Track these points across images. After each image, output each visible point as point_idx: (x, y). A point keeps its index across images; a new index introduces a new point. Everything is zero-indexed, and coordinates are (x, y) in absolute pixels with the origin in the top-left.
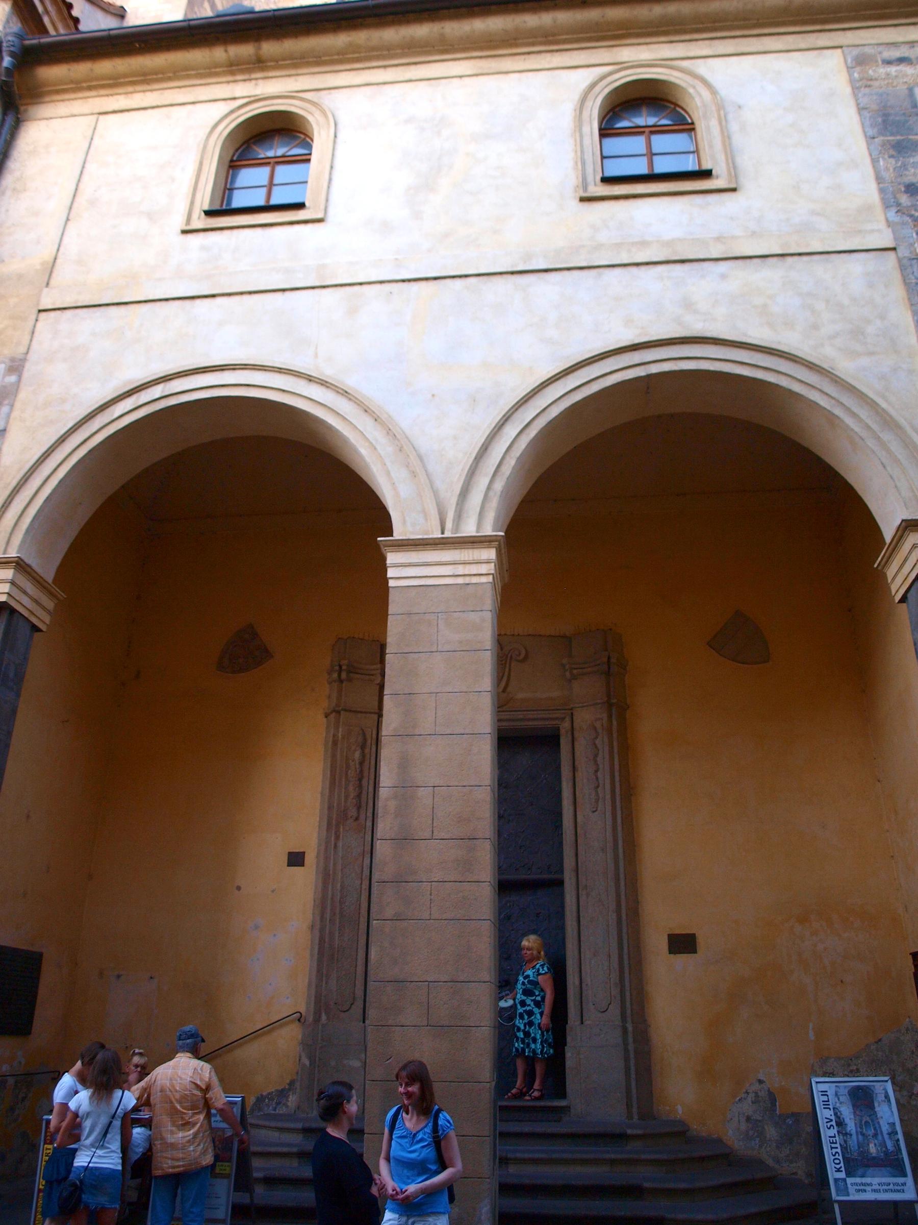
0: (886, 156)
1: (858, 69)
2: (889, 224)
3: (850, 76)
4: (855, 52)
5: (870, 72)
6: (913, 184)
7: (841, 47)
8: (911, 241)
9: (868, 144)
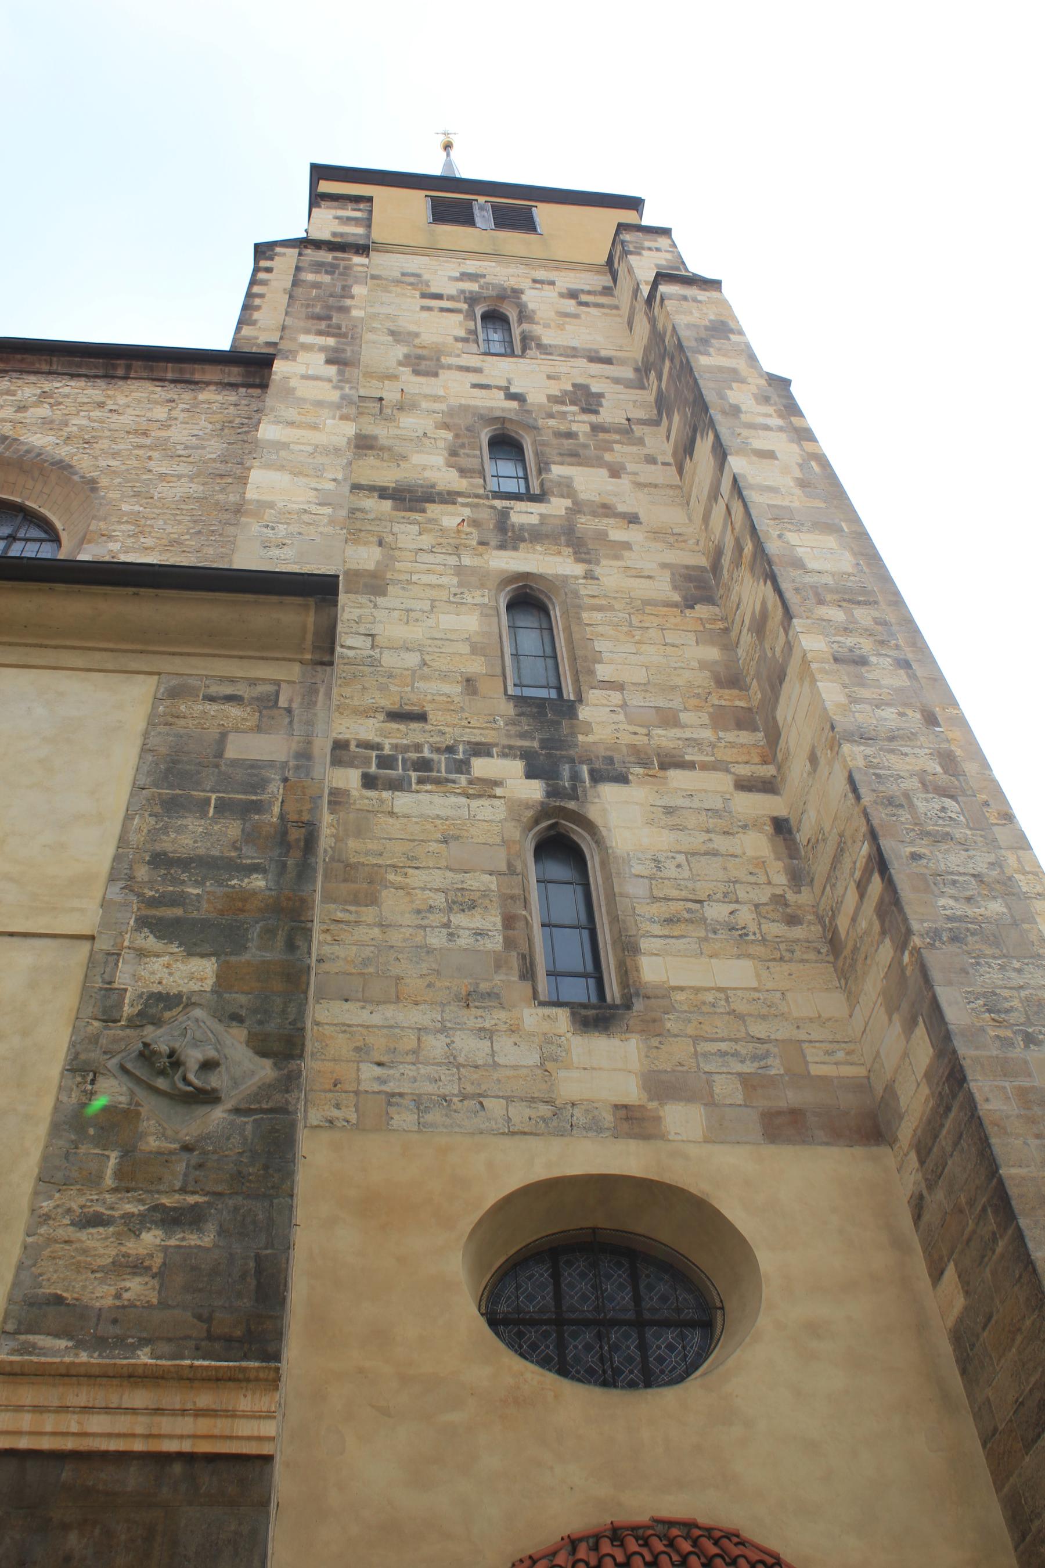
0: (146, 814)
1: (168, 702)
2: (104, 904)
3: (154, 707)
4: (174, 682)
5: (183, 708)
6: (165, 854)
7: (159, 674)
8: (124, 928)
9: (132, 795)
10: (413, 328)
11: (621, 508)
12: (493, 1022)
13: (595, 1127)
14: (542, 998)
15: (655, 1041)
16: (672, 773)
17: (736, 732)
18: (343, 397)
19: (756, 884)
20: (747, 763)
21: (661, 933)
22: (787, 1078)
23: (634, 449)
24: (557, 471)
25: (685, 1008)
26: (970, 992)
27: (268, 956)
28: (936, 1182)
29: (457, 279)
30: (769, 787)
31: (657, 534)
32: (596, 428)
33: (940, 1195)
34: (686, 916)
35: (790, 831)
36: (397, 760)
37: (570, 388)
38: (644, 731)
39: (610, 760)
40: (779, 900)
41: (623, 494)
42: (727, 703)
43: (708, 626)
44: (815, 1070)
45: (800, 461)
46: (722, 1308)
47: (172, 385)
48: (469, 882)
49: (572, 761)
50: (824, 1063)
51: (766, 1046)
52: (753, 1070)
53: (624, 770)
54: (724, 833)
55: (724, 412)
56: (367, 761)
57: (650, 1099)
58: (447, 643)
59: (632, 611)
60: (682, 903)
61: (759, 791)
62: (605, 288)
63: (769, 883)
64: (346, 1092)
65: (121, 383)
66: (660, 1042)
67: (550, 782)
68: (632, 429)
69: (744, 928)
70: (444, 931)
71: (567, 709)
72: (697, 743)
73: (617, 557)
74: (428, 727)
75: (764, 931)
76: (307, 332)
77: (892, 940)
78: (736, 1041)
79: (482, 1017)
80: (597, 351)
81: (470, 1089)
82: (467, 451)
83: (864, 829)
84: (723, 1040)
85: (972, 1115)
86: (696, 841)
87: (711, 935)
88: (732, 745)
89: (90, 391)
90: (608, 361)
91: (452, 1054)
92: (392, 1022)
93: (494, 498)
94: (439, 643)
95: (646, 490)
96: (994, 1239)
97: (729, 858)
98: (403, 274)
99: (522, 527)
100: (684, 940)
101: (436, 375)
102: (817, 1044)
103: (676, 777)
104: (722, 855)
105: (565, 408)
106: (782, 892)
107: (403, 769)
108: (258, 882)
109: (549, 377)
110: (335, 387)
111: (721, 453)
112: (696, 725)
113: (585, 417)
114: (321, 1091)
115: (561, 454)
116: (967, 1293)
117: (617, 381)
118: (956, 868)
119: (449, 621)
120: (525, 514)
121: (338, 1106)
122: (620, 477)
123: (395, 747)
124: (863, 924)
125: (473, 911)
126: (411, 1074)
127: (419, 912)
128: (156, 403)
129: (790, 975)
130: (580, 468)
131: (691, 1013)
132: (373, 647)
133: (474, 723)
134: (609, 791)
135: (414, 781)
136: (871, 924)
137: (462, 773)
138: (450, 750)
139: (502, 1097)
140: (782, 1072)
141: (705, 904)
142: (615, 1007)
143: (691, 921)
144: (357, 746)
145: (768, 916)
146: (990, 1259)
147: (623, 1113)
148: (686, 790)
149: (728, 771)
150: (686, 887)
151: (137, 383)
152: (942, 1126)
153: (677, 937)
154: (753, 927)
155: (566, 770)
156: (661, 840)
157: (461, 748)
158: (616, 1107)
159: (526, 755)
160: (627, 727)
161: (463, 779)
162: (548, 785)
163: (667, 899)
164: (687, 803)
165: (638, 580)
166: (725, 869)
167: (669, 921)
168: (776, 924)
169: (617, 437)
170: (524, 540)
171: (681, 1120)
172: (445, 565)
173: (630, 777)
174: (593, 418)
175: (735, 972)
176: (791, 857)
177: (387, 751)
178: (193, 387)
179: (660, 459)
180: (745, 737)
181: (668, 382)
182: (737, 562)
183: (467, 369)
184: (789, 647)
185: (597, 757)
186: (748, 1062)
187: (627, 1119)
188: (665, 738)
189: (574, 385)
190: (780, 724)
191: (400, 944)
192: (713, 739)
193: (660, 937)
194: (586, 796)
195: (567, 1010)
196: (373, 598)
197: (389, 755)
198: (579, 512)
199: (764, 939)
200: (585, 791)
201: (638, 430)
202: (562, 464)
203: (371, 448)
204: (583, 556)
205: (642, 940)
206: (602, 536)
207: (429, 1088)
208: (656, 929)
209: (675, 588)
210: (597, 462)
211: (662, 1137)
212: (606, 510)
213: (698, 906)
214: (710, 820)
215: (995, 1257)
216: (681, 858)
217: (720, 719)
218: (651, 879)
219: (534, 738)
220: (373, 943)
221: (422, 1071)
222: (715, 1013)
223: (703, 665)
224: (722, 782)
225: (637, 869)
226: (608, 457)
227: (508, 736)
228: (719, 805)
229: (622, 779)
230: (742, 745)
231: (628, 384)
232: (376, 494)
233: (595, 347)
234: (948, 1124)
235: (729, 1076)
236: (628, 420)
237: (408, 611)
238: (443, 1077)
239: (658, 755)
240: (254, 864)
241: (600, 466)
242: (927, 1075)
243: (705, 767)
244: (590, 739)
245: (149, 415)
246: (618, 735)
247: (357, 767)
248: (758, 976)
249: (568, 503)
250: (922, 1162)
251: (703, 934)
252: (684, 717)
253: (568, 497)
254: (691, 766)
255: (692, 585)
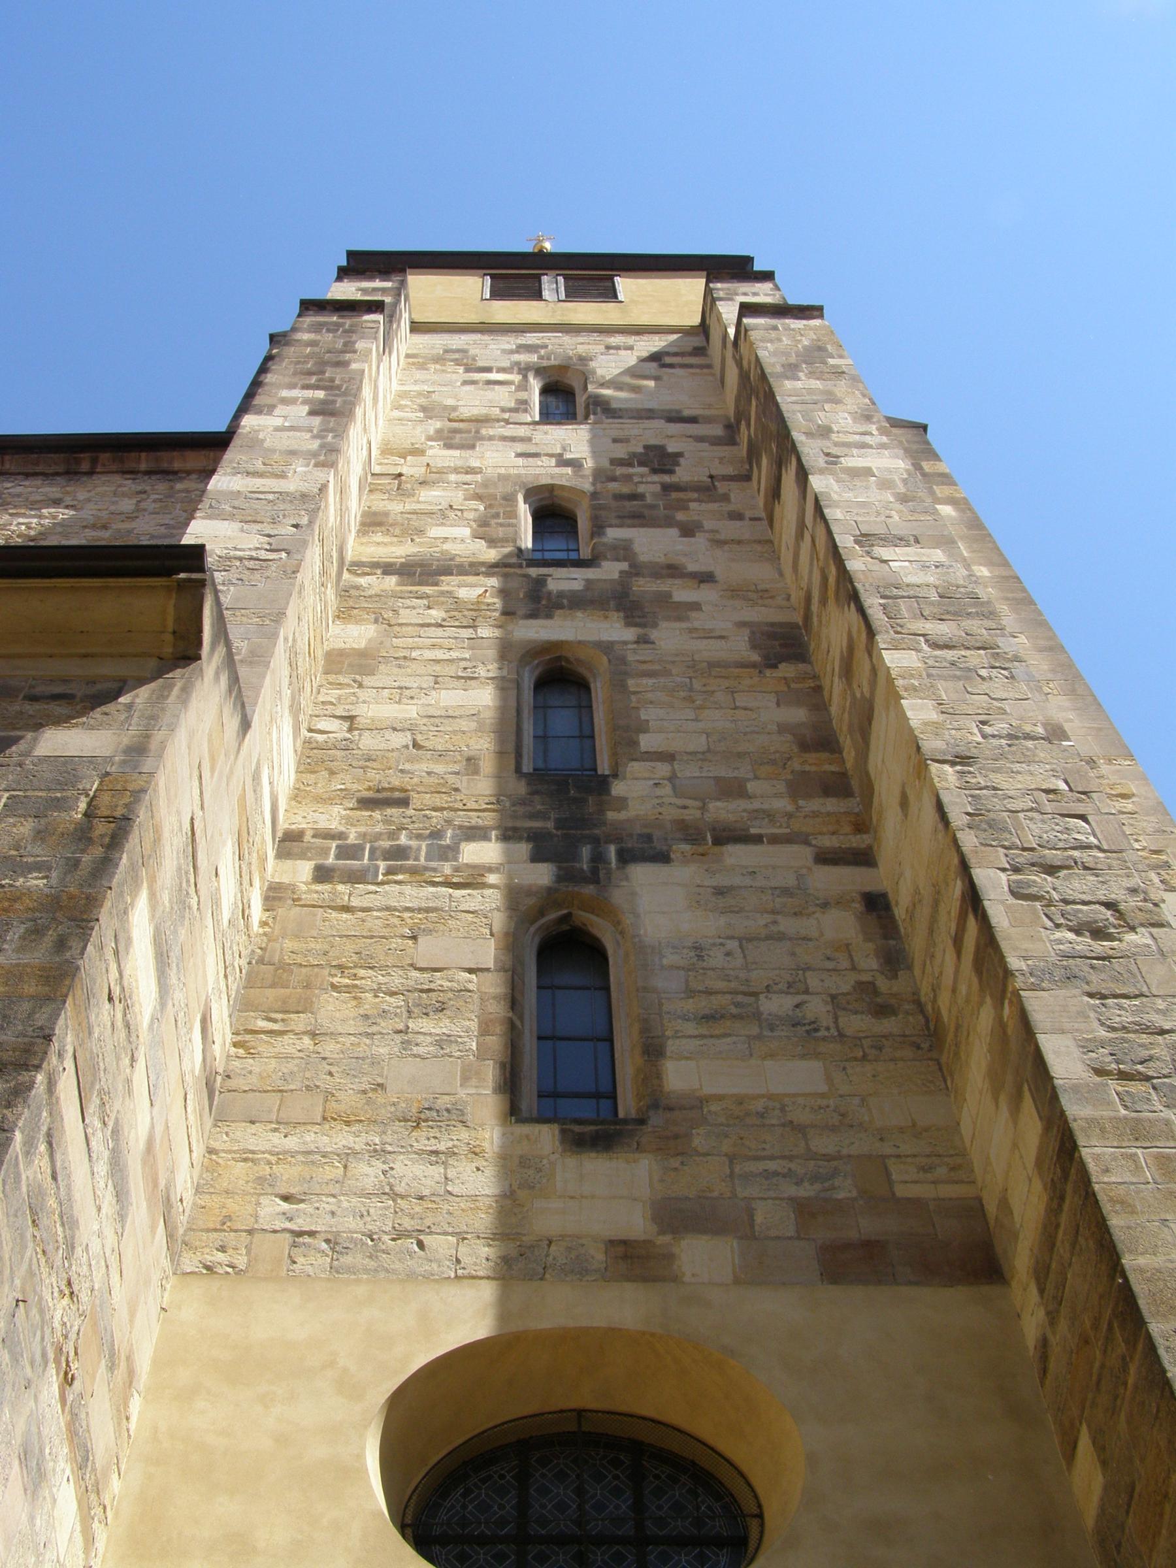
10: (450, 402)
11: (692, 567)
12: (450, 1144)
13: (578, 1269)
14: (525, 1114)
15: (675, 1162)
16: (730, 848)
17: (821, 800)
18: (322, 446)
19: (834, 970)
20: (833, 833)
21: (696, 1033)
22: (861, 1202)
23: (714, 506)
24: (613, 534)
25: (722, 1120)
26: (1090, 1040)
27: (26, 958)
28: (1058, 1311)
29: (512, 352)
30: (864, 858)
31: (736, 592)
32: (667, 488)
33: (1063, 1325)
34: (734, 1010)
35: (887, 907)
36: (363, 849)
37: (642, 450)
38: (698, 804)
39: (649, 838)
40: (866, 988)
41: (697, 554)
42: (813, 768)
43: (793, 686)
44: (901, 1191)
45: (905, 476)
46: (760, 1516)
47: (146, 478)
48: (439, 982)
49: (596, 841)
50: (916, 1182)
51: (835, 1163)
52: (812, 1194)
53: (665, 848)
54: (795, 914)
55: (809, 434)
56: (325, 852)
57: (662, 1232)
58: (446, 721)
59: (692, 674)
60: (728, 997)
61: (847, 863)
62: (696, 349)
63: (854, 968)
64: (236, 1231)
65: (85, 479)
66: (682, 1163)
67: (565, 865)
68: (714, 486)
69: (814, 1022)
70: (398, 1038)
71: (601, 785)
72: (770, 816)
73: (679, 619)
74: (410, 812)
75: (841, 1025)
76: (292, 386)
77: (991, 997)
78: (791, 1158)
79: (435, 1138)
80: (679, 411)
81: (408, 1224)
82: (501, 521)
83: (956, 861)
84: (772, 1158)
85: (1087, 1193)
86: (758, 923)
87: (766, 1033)
88: (815, 814)
89: (47, 489)
90: (693, 420)
91: (390, 1184)
92: (312, 1147)
93: (528, 566)
94: (437, 721)
95: (726, 547)
96: (1125, 1368)
97: (800, 942)
98: (446, 351)
99: (561, 594)
100: (729, 1040)
101: (473, 447)
102: (909, 1160)
103: (737, 855)
104: (790, 939)
105: (631, 470)
106: (870, 979)
107: (370, 859)
108: (36, 882)
109: (615, 441)
110: (314, 437)
111: (803, 475)
112: (769, 796)
113: (656, 478)
114: (202, 1230)
115: (619, 517)
116: (1104, 1463)
117: (700, 439)
118: (1081, 896)
119: (450, 698)
120: (564, 580)
121: (222, 1249)
122: (694, 536)
123: (363, 836)
124: (963, 989)
125: (440, 1015)
126: (328, 1208)
127: (366, 1017)
128: (124, 495)
129: (874, 1076)
130: (642, 530)
131: (728, 1126)
132: (350, 730)
133: (469, 806)
134: (641, 873)
135: (381, 871)
136: (970, 986)
137: (447, 860)
138: (436, 834)
139: (452, 1234)
140: (854, 1194)
141: (762, 997)
142: (625, 1121)
143: (739, 1017)
144: (313, 836)
145: (850, 1007)
146: (1123, 1399)
147: (621, 1250)
148: (746, 867)
149: (807, 843)
150: (737, 977)
151: (104, 478)
152: (1058, 1226)
153: (718, 1037)
154: (826, 1020)
155: (586, 851)
156: (707, 925)
157: (449, 833)
158: (612, 1243)
159: (535, 837)
160: (674, 800)
161: (447, 868)
162: (559, 868)
163: (709, 992)
164: (748, 881)
165: (705, 642)
166: (793, 954)
167: (709, 1018)
168: (859, 1017)
169: (696, 495)
170: (561, 607)
171: (702, 1258)
172: (456, 638)
173: (672, 856)
174: (666, 478)
175: (795, 1077)
176: (886, 937)
177: (352, 839)
178: (171, 477)
179: (748, 514)
180: (831, 805)
181: (756, 429)
182: (824, 602)
183: (513, 439)
184: (874, 671)
185: (631, 835)
186: (806, 1184)
187: (625, 1257)
188: (723, 811)
189: (646, 447)
190: (873, 778)
191: (336, 1056)
192: (790, 808)
193: (695, 1037)
194: (609, 879)
195: (556, 1128)
196: (358, 677)
197: (354, 845)
198: (637, 575)
199: (841, 1035)
200: (609, 872)
201: (722, 487)
202: (621, 526)
203: (380, 524)
204: (638, 620)
205: (670, 1042)
206: (664, 599)
207: (352, 1223)
208: (690, 1028)
209: (754, 646)
210: (669, 522)
211: (675, 1279)
212: (673, 570)
213: (753, 999)
214: (778, 900)
215: (1128, 1393)
216: (733, 945)
217: (799, 787)
218: (689, 970)
219: (549, 818)
220: (301, 1055)
221: (345, 1204)
222: (764, 1125)
223: (782, 728)
224: (801, 855)
225: (670, 958)
226: (680, 516)
227: (514, 817)
228: (791, 881)
229: (663, 858)
230: (829, 814)
231: (716, 441)
232: (379, 571)
233: (677, 407)
234: (1064, 1218)
235: (777, 1202)
236: (711, 477)
237: (400, 688)
238: (372, 1211)
239: (714, 829)
240: (36, 863)
241: (670, 525)
242: (1039, 1163)
243: (775, 840)
244: (623, 816)
245: (113, 508)
246: (660, 810)
247: (309, 859)
248: (829, 1079)
249: (624, 566)
250: (1041, 1291)
251: (755, 1030)
252: (751, 787)
253: (625, 560)
254: (758, 839)
255: (777, 643)
